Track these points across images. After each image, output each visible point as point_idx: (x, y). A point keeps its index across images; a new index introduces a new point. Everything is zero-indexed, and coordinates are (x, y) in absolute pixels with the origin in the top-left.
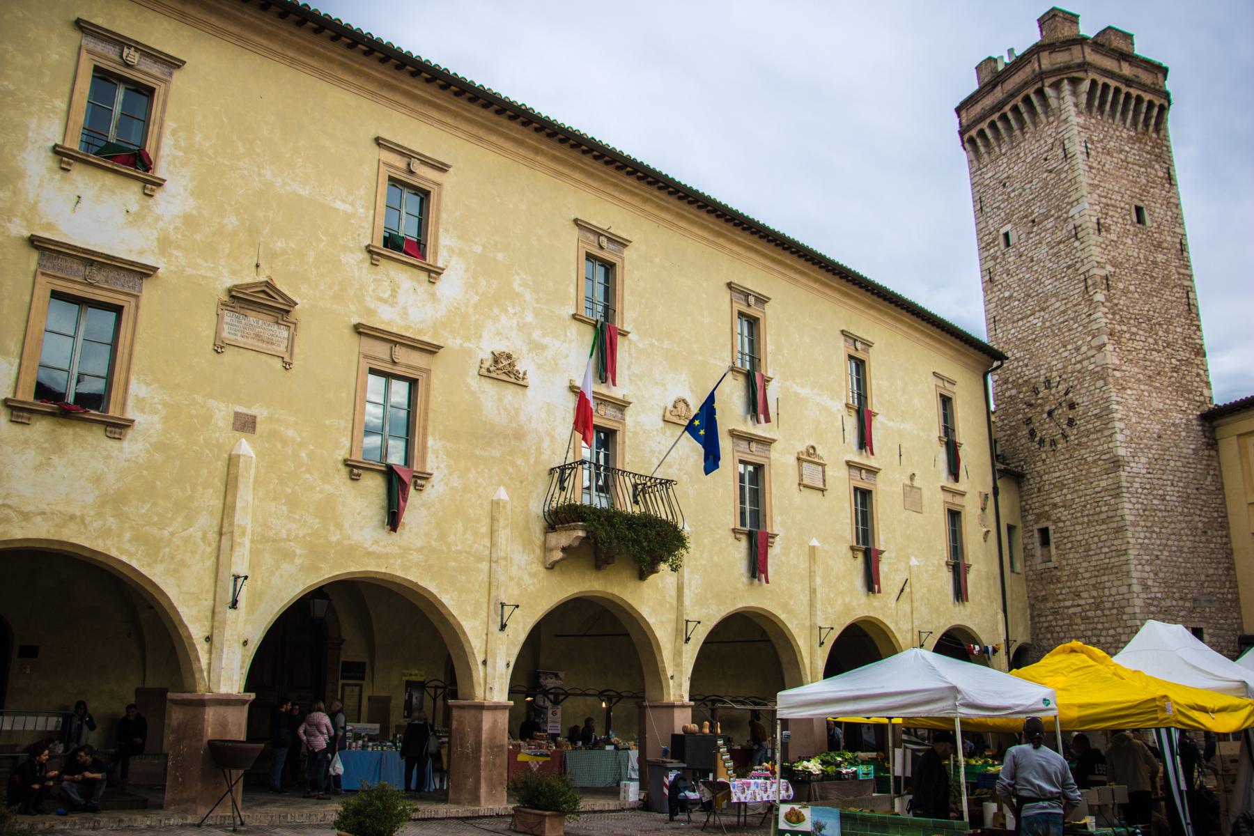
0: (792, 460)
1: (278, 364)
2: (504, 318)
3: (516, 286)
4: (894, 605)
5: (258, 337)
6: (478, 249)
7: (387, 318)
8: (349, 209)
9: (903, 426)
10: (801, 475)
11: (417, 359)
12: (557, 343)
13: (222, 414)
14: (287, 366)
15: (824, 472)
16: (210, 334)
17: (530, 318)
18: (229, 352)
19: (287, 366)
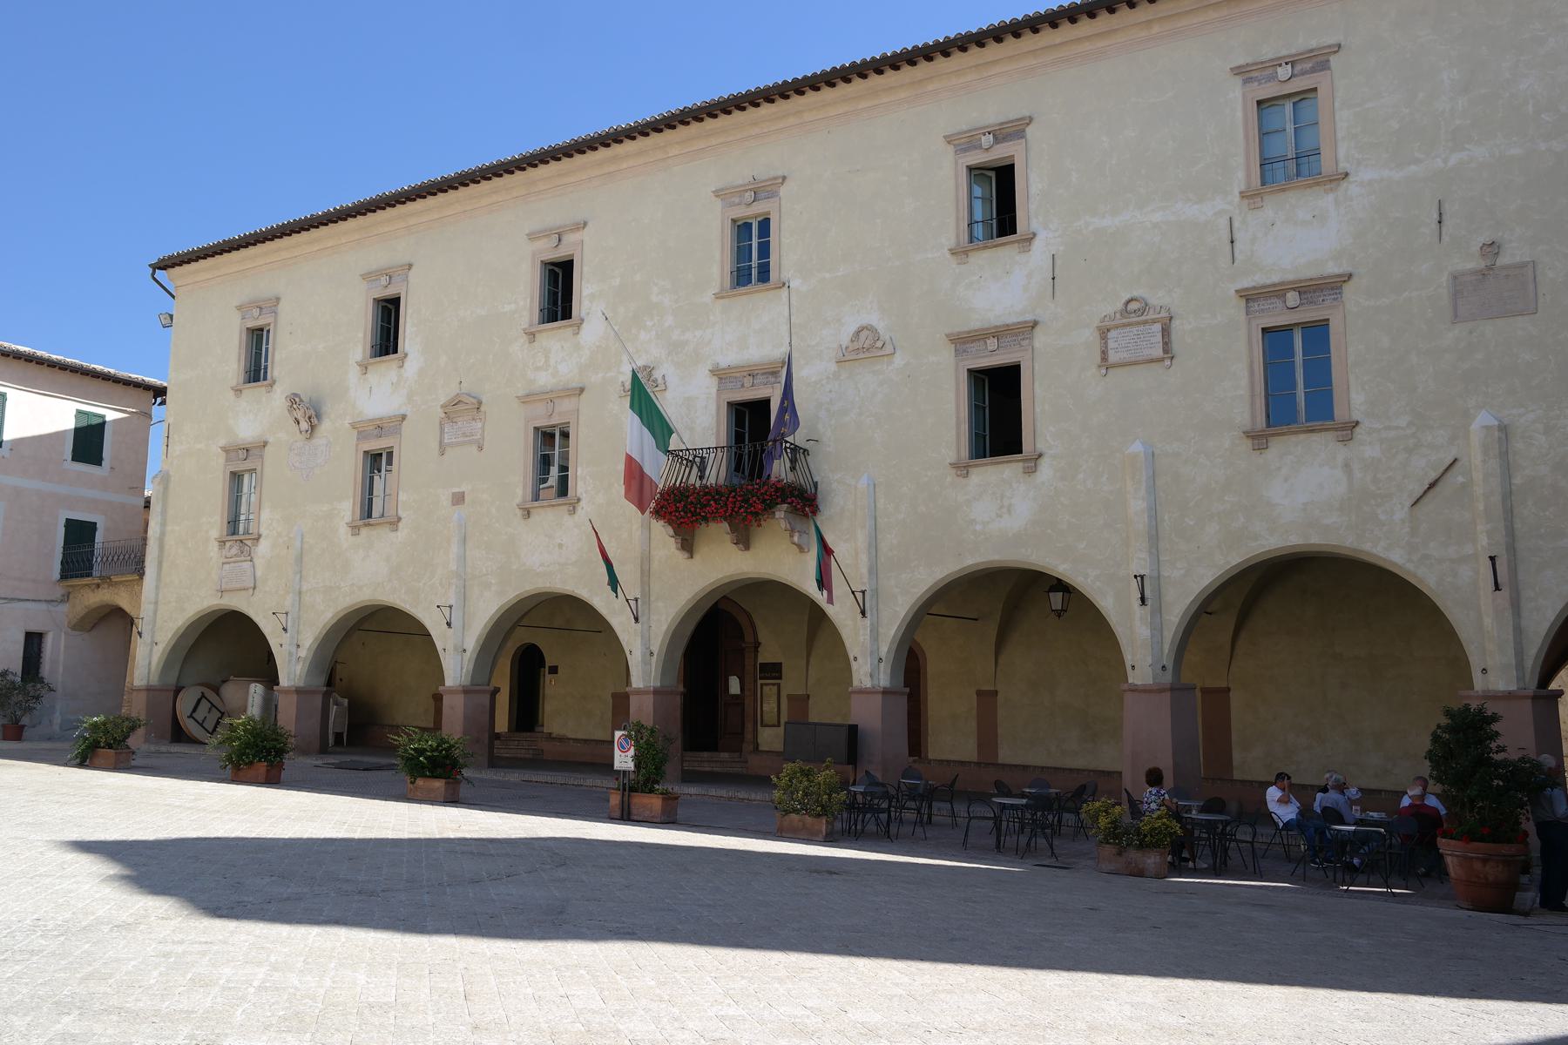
0: (1089, 335)
1: (474, 448)
2: (643, 336)
3: (654, 299)
4: (1401, 512)
5: (464, 434)
6: (617, 281)
7: (544, 380)
8: (513, 306)
9: (1454, 159)
10: (1104, 354)
11: (566, 405)
12: (698, 333)
13: (445, 498)
14: (481, 448)
15: (1166, 332)
16: (435, 445)
17: (669, 320)
18: (448, 450)
19: (481, 448)
